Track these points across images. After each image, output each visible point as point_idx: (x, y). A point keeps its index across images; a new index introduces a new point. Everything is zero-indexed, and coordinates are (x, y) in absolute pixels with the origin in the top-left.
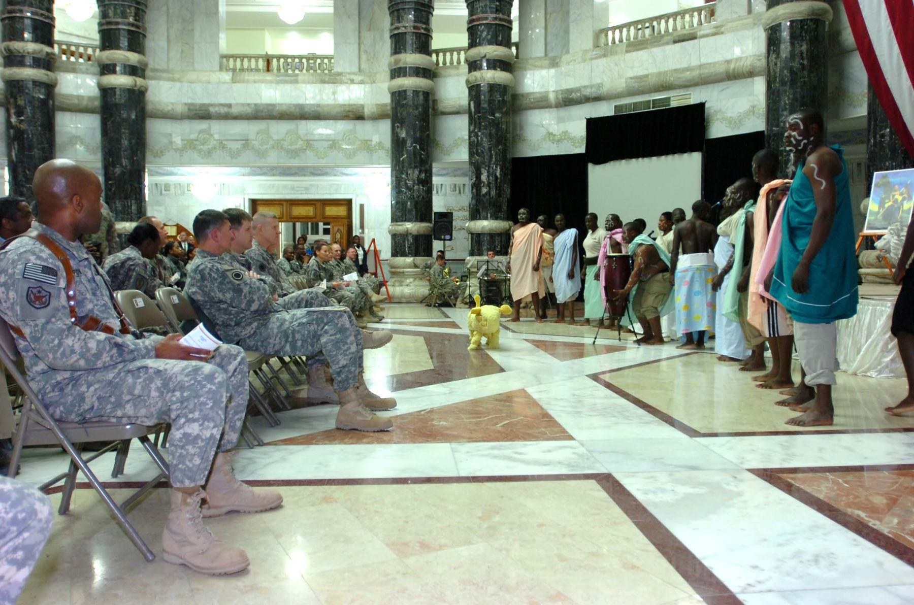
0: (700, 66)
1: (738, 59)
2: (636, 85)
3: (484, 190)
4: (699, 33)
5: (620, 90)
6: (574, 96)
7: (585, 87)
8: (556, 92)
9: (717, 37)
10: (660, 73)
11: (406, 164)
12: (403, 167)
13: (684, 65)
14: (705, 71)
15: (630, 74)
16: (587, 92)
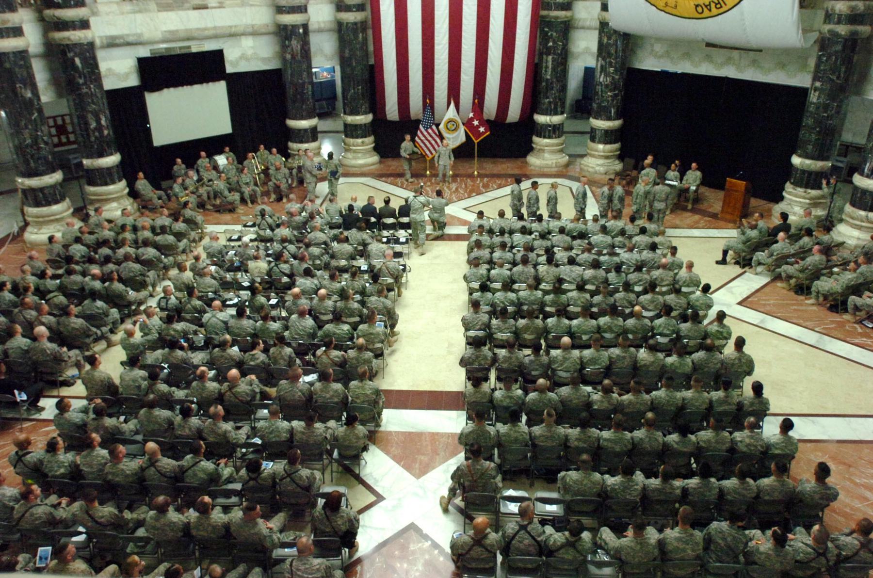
0: (215, 28)
1: (236, 26)
2: (168, 36)
3: (106, 132)
4: (209, 5)
5: (157, 39)
6: (118, 41)
7: (128, 35)
8: (101, 37)
9: (222, 9)
10: (187, 30)
11: (39, 122)
12: (36, 125)
13: (202, 25)
14: (218, 32)
15: (164, 29)
16: (131, 39)
